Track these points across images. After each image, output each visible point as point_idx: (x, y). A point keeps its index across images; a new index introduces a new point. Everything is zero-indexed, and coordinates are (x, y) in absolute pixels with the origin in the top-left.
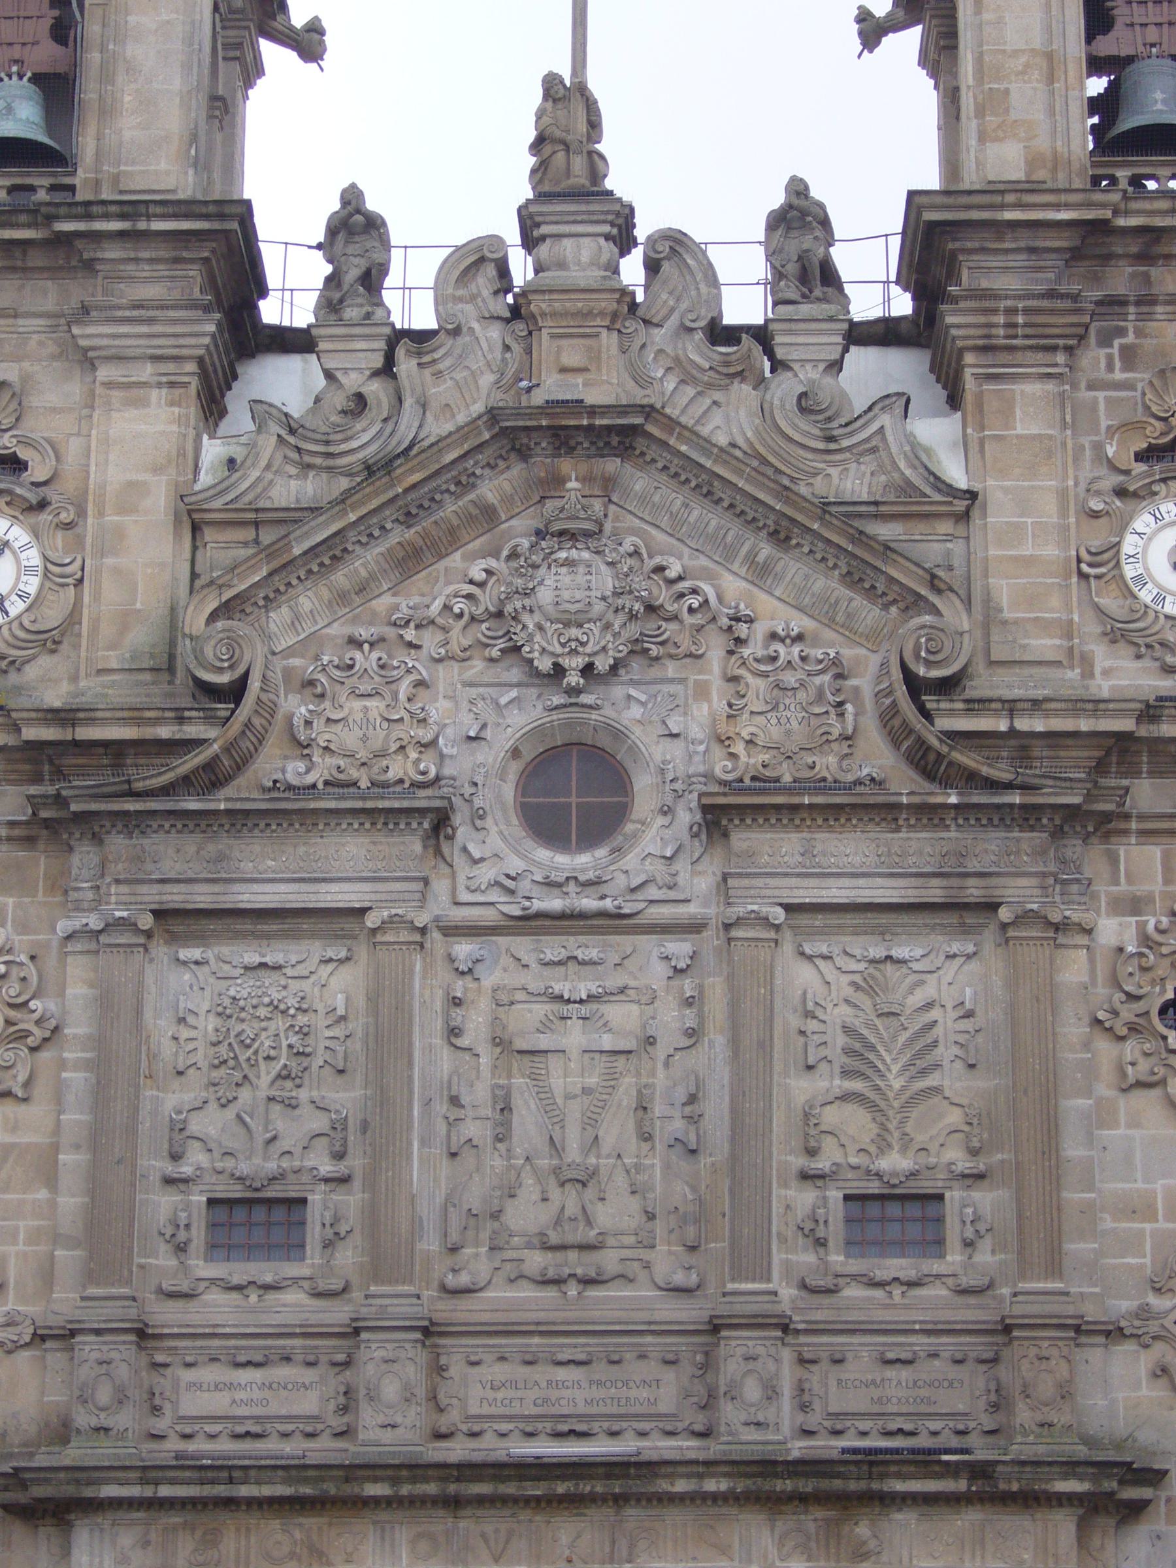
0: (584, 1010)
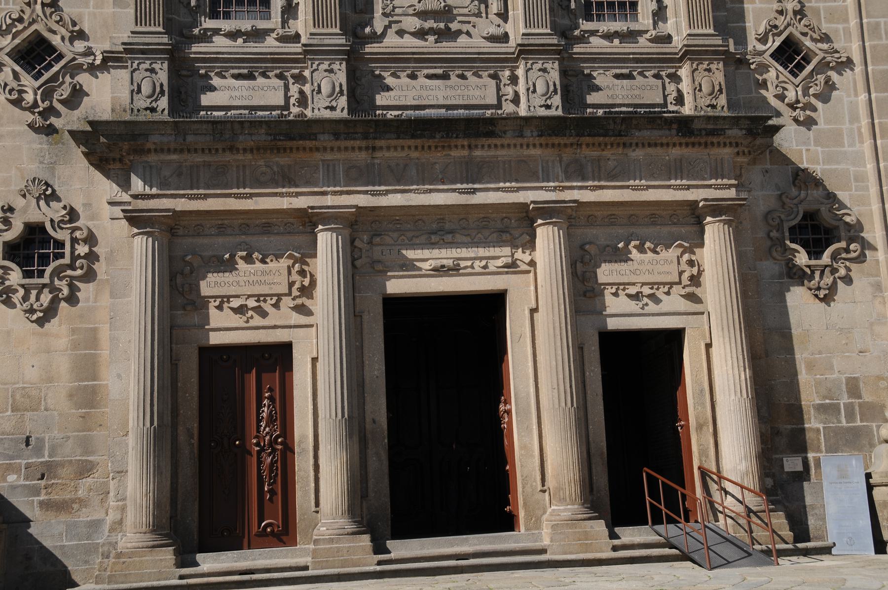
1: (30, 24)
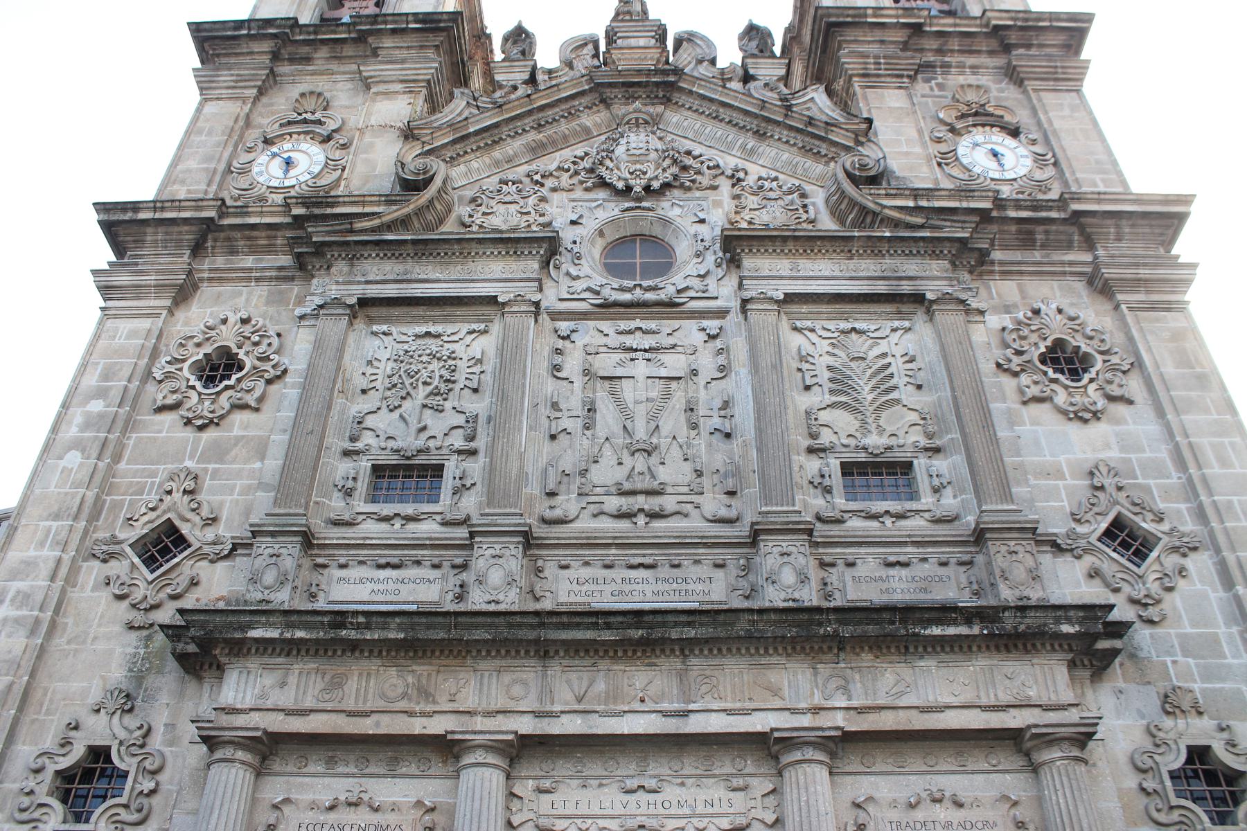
0: (647, 355)
1: (165, 512)
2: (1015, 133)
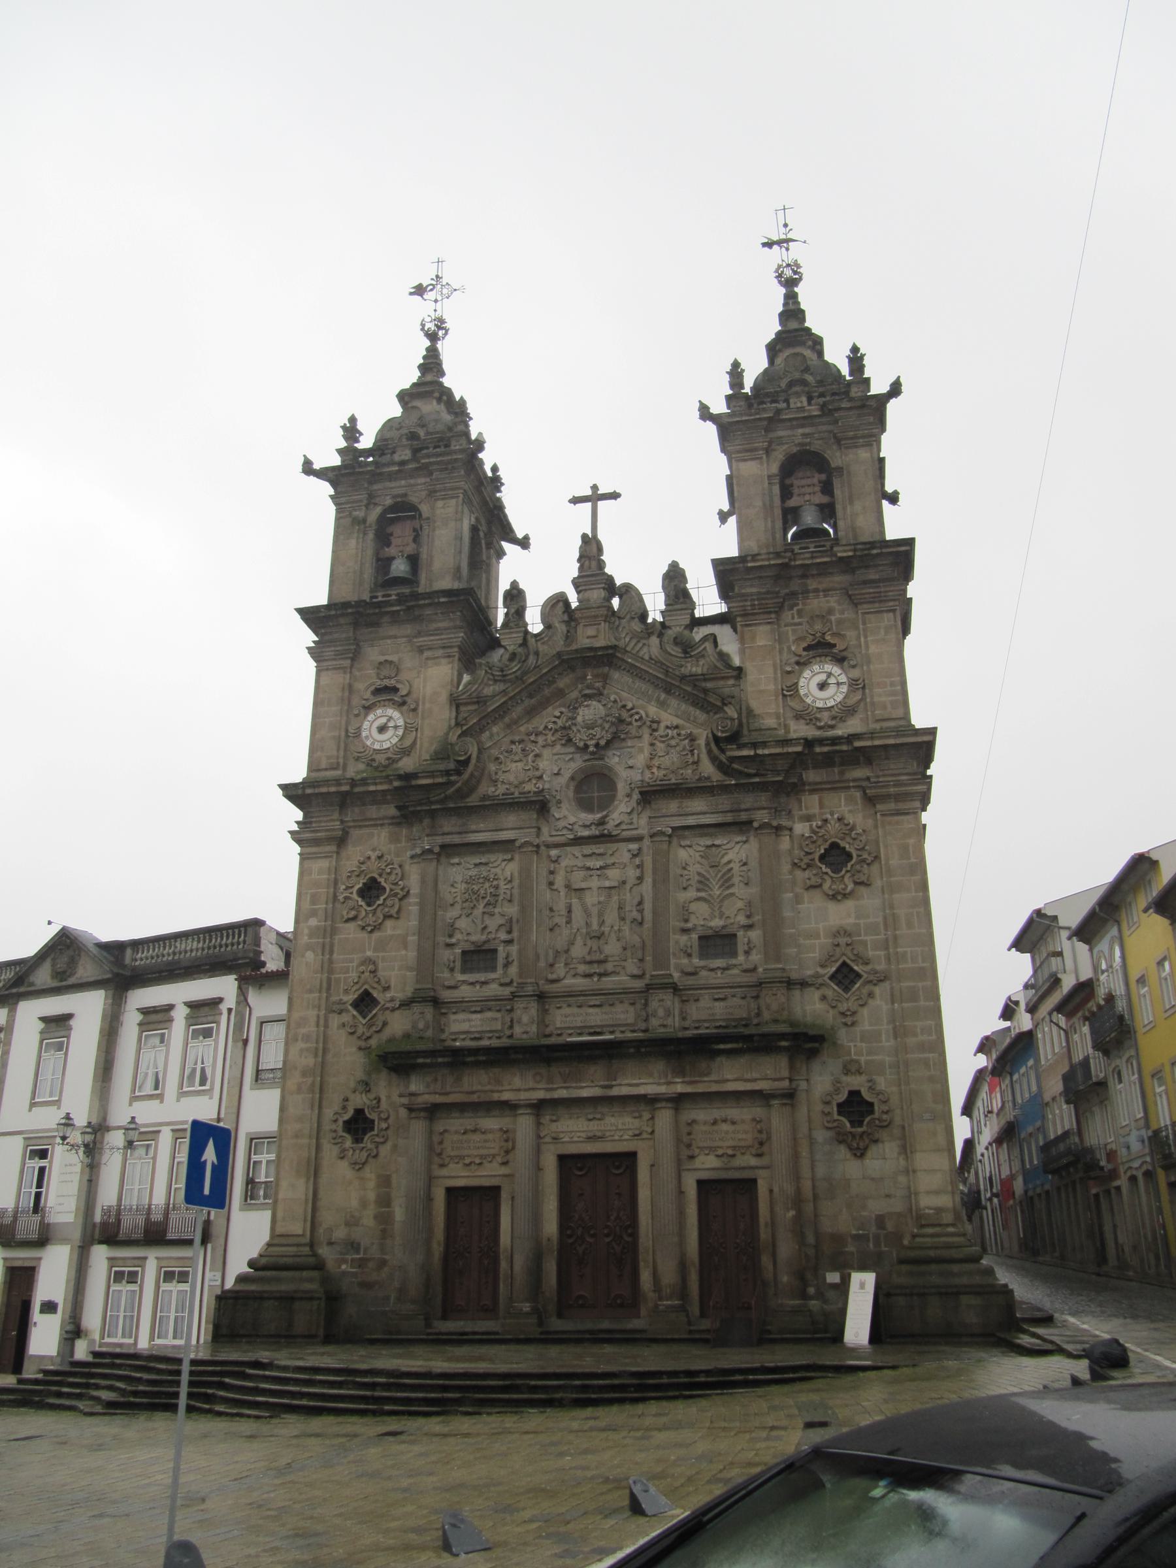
0: (599, 872)
2: (840, 660)
